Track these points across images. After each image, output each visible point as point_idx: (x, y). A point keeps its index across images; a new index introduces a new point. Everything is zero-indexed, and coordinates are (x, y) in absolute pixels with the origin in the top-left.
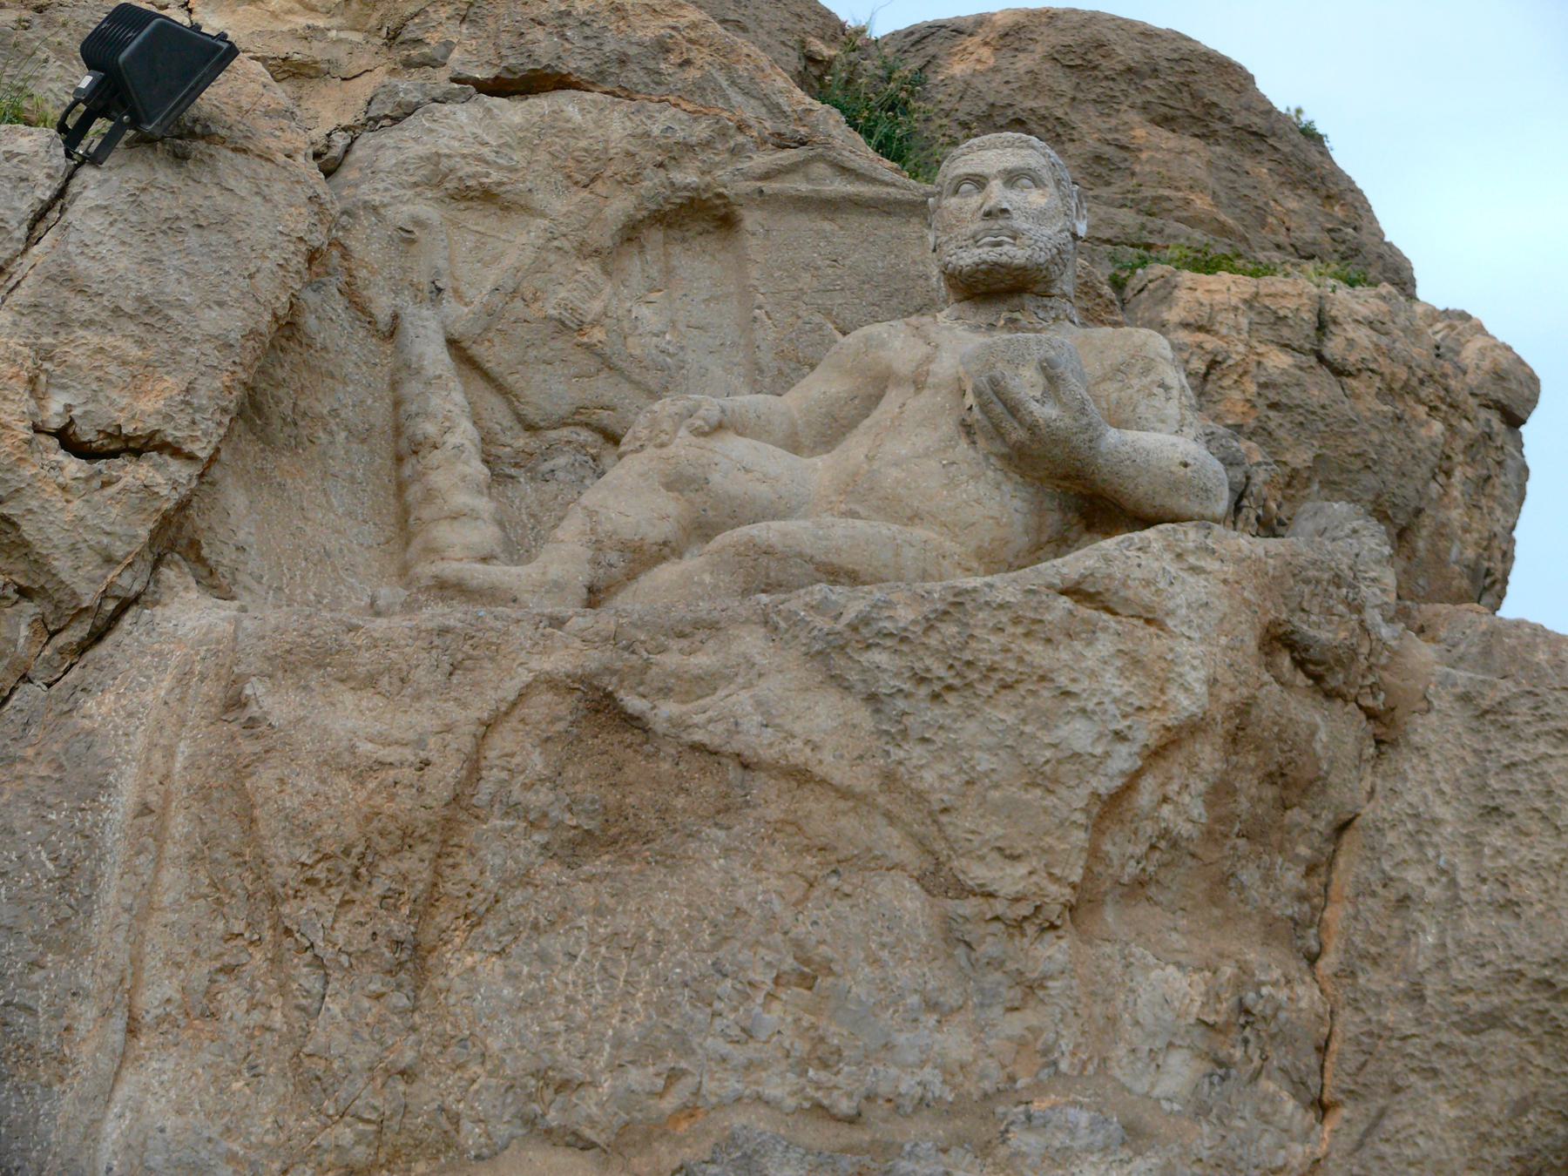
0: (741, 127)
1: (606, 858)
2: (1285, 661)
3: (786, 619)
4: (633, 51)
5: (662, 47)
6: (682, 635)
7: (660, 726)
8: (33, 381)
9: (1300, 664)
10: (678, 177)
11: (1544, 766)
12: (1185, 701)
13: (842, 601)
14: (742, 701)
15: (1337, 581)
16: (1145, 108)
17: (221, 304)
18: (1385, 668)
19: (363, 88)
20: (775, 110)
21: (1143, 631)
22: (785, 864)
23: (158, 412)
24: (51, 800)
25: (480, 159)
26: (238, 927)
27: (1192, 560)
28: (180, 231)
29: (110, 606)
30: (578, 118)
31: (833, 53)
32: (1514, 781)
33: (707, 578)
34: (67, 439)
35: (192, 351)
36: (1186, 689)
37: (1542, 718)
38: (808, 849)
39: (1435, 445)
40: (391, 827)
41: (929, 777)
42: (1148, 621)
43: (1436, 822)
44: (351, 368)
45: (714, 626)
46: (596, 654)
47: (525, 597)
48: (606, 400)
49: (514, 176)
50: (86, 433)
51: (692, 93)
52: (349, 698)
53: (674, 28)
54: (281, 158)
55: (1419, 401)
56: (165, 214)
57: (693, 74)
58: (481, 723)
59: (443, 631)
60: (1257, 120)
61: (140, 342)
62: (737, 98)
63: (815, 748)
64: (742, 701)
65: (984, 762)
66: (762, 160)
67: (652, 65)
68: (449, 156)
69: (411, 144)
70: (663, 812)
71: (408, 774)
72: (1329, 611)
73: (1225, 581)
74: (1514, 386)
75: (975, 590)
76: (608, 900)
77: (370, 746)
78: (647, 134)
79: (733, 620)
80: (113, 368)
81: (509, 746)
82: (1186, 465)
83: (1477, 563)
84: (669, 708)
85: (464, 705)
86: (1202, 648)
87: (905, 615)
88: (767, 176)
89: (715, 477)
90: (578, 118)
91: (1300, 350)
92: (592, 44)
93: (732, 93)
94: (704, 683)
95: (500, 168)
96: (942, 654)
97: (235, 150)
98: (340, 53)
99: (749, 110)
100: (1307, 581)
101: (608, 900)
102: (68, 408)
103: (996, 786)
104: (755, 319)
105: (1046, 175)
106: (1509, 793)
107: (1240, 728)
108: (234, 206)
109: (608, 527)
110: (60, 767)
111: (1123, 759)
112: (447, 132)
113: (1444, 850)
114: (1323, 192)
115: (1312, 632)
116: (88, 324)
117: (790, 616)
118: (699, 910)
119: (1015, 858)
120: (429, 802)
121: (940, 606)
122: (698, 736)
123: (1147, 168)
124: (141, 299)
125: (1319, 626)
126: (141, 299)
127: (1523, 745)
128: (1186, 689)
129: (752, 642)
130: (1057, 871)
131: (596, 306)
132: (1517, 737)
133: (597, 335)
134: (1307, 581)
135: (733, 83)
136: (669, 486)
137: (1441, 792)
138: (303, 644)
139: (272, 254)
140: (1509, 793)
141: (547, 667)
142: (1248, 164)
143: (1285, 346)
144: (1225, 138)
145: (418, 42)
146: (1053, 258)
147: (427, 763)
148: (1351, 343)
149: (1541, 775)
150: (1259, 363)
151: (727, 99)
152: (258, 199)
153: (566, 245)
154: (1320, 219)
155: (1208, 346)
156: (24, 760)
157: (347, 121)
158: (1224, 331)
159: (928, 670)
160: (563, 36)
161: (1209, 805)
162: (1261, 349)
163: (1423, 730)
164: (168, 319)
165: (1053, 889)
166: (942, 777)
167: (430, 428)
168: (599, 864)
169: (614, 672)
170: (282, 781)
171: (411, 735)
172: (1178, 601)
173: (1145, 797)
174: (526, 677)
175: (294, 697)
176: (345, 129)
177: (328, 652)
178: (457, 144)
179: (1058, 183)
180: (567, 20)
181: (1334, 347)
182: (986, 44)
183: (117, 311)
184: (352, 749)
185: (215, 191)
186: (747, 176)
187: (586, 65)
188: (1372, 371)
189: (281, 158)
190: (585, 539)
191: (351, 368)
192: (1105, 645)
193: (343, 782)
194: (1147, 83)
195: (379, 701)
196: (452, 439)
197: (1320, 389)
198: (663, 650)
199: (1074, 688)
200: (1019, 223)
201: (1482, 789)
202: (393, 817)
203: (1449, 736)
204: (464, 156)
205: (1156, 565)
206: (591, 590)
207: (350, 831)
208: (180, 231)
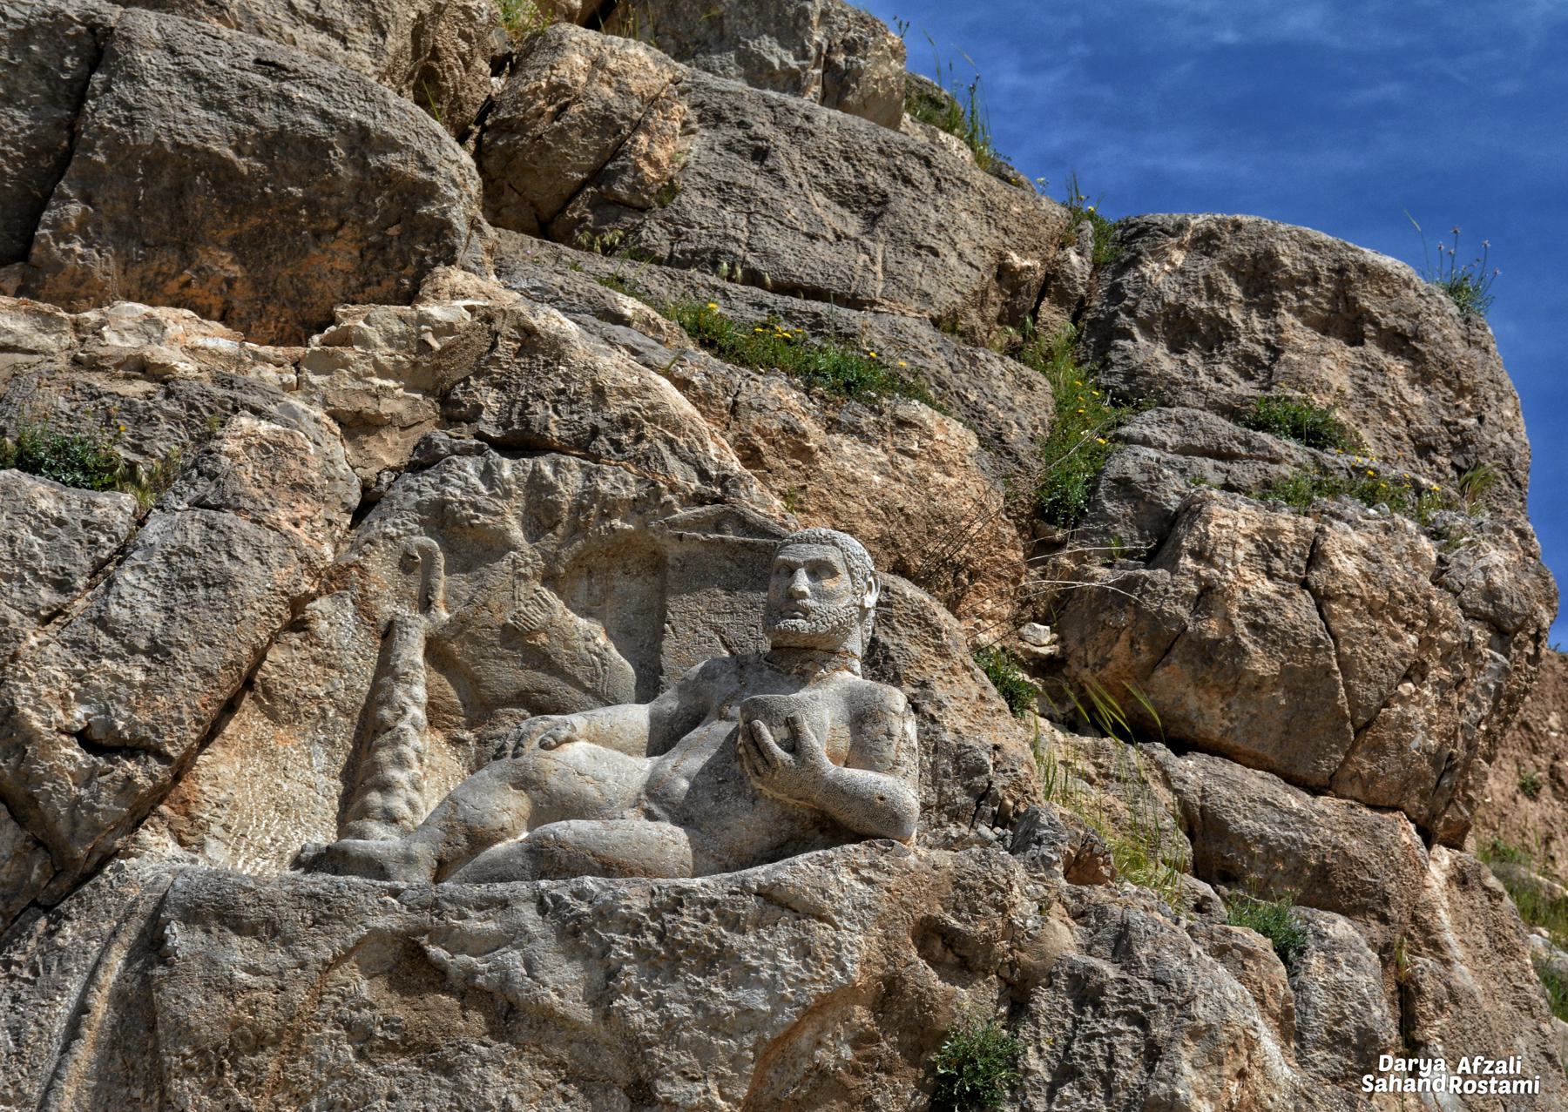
0: (673, 489)
1: (402, 1060)
2: (938, 945)
3: (554, 902)
4: (602, 425)
5: (625, 422)
6: (479, 908)
7: (453, 970)
8: (64, 697)
9: (949, 946)
10: (617, 523)
11: (1115, 1040)
12: (837, 974)
13: (597, 890)
14: (513, 959)
15: (991, 887)
16: (1300, 312)
17: (211, 644)
18: (1021, 950)
19: (414, 437)
20: (703, 475)
21: (814, 924)
22: (528, 1071)
23: (147, 724)
24: (24, 996)
25: (474, 506)
26: (138, 1093)
27: (864, 873)
28: (193, 587)
29: (96, 858)
30: (552, 478)
31: (1027, 263)
32: (1089, 1049)
33: (519, 861)
34: (85, 739)
35: (183, 679)
36: (843, 970)
37: (1125, 1002)
38: (542, 1065)
39: (1404, 655)
40: (249, 1032)
41: (638, 1019)
42: (821, 919)
43: (1027, 1072)
44: (350, 661)
45: (504, 904)
46: (415, 917)
47: (392, 867)
48: (542, 687)
49: (498, 518)
50: (98, 734)
51: (639, 461)
52: (235, 940)
53: (638, 409)
54: (287, 526)
55: (1398, 619)
56: (185, 574)
57: (645, 445)
58: (325, 962)
59: (312, 896)
60: (1404, 323)
61: (147, 670)
62: (672, 462)
63: (561, 995)
64: (513, 959)
65: (681, 1011)
66: (681, 513)
67: (615, 436)
68: (451, 502)
69: (429, 489)
70: (447, 1032)
71: (268, 997)
72: (974, 910)
73: (888, 890)
74: (1505, 602)
75: (691, 890)
76: (397, 1090)
77: (244, 975)
78: (597, 492)
79: (516, 898)
80: (122, 689)
81: (344, 978)
82: (882, 799)
83: (1439, 750)
84: (464, 958)
85: (315, 947)
86: (861, 938)
87: (639, 904)
88: (686, 524)
89: (553, 780)
90: (552, 478)
91: (1287, 578)
92: (576, 417)
93: (672, 462)
94: (488, 945)
95: (486, 511)
96: (661, 936)
97: (253, 521)
98: (400, 407)
99: (681, 474)
100: (963, 889)
101: (397, 1090)
102: (87, 716)
103: (687, 1029)
104: (664, 631)
105: (840, 567)
106: (1083, 1057)
107: (889, 994)
108: (235, 568)
109: (461, 816)
110: (36, 974)
111: (788, 1015)
112: (455, 481)
113: (1029, 1092)
114: (1456, 385)
115: (959, 925)
116: (113, 657)
117: (556, 899)
118: (459, 1102)
119: (693, 1080)
120: (278, 1015)
121: (665, 899)
122: (480, 980)
123: (1284, 369)
124: (152, 640)
125: (967, 921)
126: (152, 640)
127: (1104, 1021)
128: (843, 970)
129: (528, 914)
130: (727, 1090)
131: (542, 617)
132: (1103, 1015)
133: (543, 638)
134: (963, 889)
135: (674, 452)
136: (515, 786)
137: (1040, 1050)
138: (209, 901)
139: (257, 605)
140: (1083, 1057)
141: (379, 925)
142: (1388, 360)
143: (1270, 574)
144: (1370, 338)
145: (459, 404)
146: (834, 628)
147: (283, 989)
148: (1334, 573)
149: (1111, 1046)
150: (1245, 590)
151: (664, 466)
152: (257, 563)
153: (529, 571)
154: (1441, 411)
155: (1203, 573)
156: (18, 964)
157: (393, 462)
158: (1220, 561)
159: (649, 944)
160: (556, 411)
161: (855, 1047)
162: (1249, 576)
163: (1043, 1000)
164: (169, 654)
165: (719, 1101)
166: (647, 1021)
167: (386, 713)
168: (396, 1063)
169: (425, 932)
170: (178, 997)
171: (273, 969)
172: (846, 903)
173: (803, 1042)
174: (365, 932)
175: (199, 936)
176: (392, 470)
177: (226, 908)
178: (458, 492)
179: (850, 571)
180: (562, 398)
181: (1318, 577)
182: (1180, 246)
183: (133, 650)
184: (231, 979)
185: (224, 557)
186: (672, 525)
187: (565, 433)
188: (1353, 596)
189: (287, 526)
190: (443, 823)
191: (350, 661)
192: (783, 934)
193: (220, 999)
194: (1308, 290)
195: (255, 943)
196: (401, 725)
197: (1300, 612)
198: (462, 916)
199: (754, 963)
200: (810, 602)
201: (1067, 1048)
202: (252, 1027)
203: (1059, 1007)
204: (461, 503)
205: (832, 877)
206: (441, 863)
207: (223, 1035)
208: (193, 587)
